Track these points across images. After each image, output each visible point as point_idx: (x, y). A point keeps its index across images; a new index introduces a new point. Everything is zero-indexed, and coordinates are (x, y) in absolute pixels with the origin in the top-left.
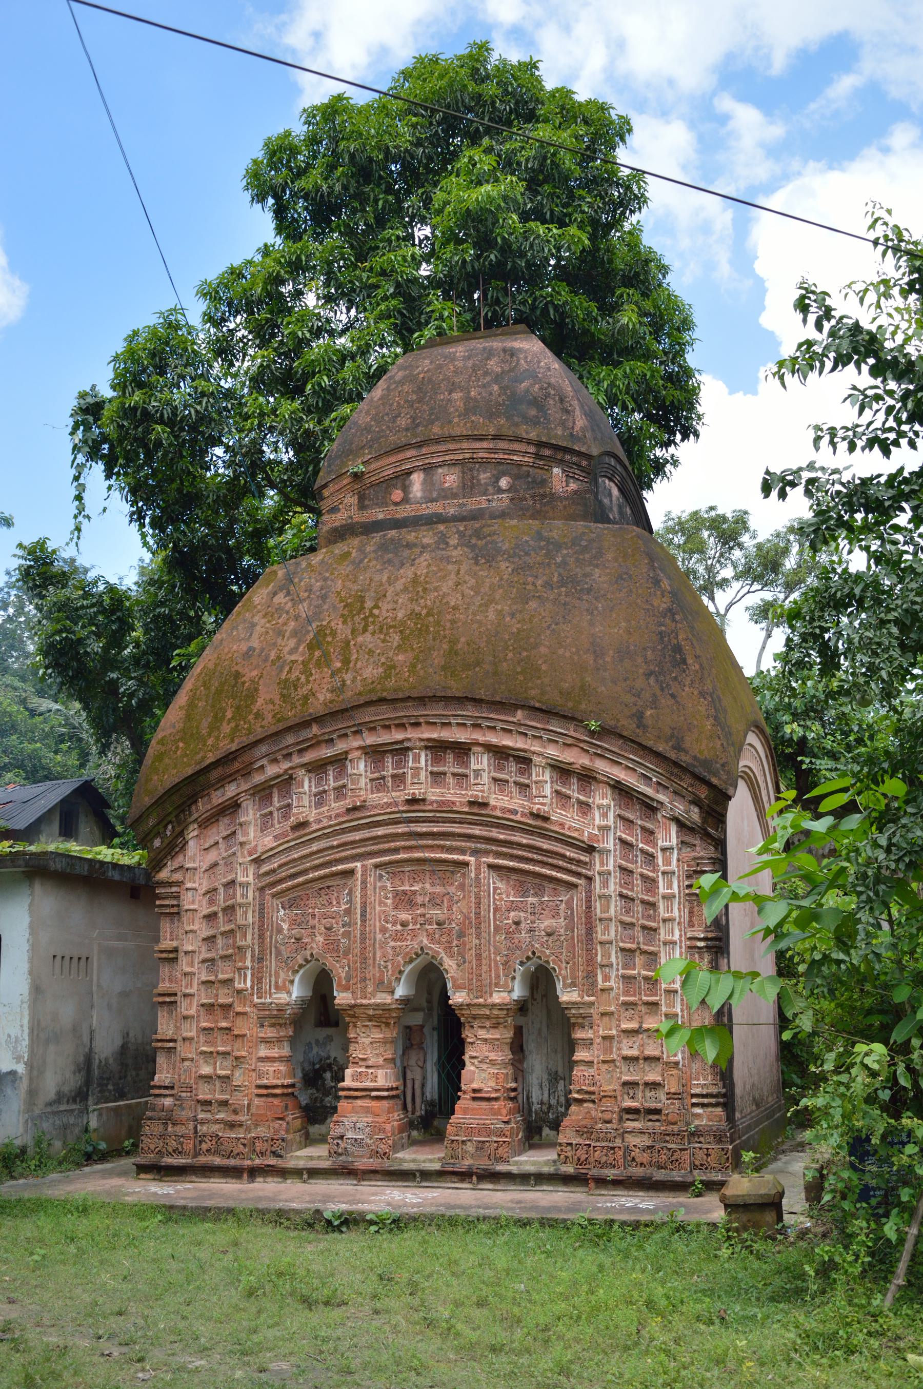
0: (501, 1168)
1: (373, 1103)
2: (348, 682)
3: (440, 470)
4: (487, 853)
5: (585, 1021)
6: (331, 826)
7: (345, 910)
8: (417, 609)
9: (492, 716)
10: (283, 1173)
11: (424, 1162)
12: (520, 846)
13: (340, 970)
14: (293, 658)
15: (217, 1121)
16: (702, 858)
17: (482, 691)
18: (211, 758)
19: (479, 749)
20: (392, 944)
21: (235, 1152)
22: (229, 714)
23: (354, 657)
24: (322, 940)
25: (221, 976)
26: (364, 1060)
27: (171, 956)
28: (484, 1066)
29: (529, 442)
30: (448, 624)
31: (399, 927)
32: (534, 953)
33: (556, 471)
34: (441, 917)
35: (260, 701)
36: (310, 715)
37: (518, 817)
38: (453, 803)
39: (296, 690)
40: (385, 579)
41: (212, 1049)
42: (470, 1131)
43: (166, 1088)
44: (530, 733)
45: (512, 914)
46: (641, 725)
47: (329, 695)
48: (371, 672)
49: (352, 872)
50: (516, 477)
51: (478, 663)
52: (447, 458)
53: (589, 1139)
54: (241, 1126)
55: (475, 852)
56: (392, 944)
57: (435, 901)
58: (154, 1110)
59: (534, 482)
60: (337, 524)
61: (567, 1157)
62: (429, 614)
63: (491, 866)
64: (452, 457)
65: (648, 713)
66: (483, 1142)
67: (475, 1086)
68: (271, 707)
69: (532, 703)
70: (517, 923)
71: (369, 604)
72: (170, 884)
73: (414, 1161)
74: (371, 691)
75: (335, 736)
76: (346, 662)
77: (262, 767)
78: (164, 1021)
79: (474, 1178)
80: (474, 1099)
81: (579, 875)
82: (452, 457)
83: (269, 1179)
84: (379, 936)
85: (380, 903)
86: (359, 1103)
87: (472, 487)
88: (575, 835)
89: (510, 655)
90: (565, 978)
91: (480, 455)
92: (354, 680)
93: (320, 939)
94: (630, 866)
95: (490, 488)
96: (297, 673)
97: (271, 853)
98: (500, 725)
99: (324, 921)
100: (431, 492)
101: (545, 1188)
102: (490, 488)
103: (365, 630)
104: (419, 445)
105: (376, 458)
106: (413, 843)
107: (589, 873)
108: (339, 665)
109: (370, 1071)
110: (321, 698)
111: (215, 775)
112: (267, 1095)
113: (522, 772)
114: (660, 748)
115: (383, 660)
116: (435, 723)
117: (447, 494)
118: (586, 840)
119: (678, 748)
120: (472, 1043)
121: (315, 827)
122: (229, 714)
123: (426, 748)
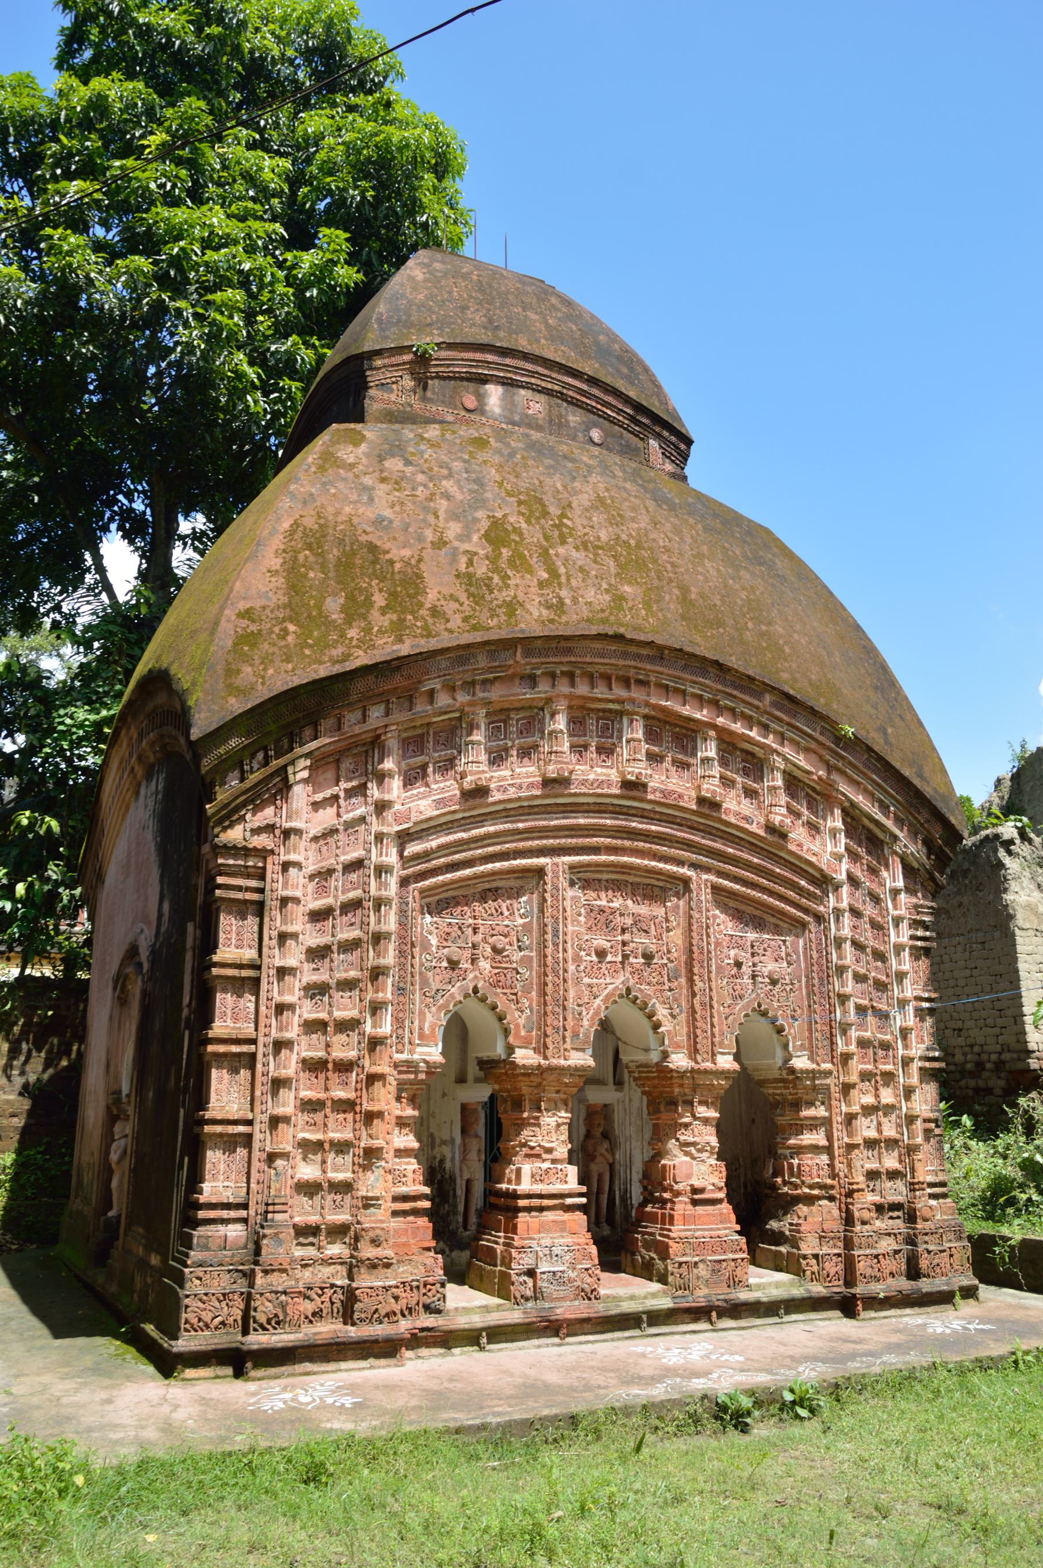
0: (743, 1295)
1: (567, 1216)
2: (568, 601)
3: (522, 392)
4: (708, 869)
5: (820, 1094)
6: (520, 799)
7: (524, 925)
8: (624, 537)
9: (735, 693)
10: (447, 1340)
11: (645, 1298)
12: (748, 866)
13: (517, 1014)
14: (466, 546)
15: (328, 1262)
16: (922, 906)
17: (733, 658)
18: (361, 659)
19: (712, 733)
20: (586, 980)
21: (383, 1312)
22: (379, 600)
23: (562, 570)
24: (488, 966)
25: (338, 1014)
26: (549, 1151)
27: (245, 973)
28: (705, 1155)
29: (627, 400)
30: (669, 567)
31: (594, 958)
32: (759, 1005)
33: (653, 443)
34: (653, 948)
35: (431, 597)
36: (522, 631)
37: (753, 828)
38: (681, 796)
39: (491, 592)
40: (559, 486)
41: (319, 1136)
42: (700, 1246)
43: (227, 1206)
44: (772, 725)
45: (732, 953)
46: (887, 742)
47: (545, 612)
48: (595, 597)
49: (540, 872)
50: (607, 434)
51: (720, 624)
52: (533, 381)
53: (835, 1246)
54: (388, 1266)
55: (694, 866)
56: (586, 980)
57: (640, 925)
58: (206, 1248)
59: (628, 446)
60: (394, 407)
61: (813, 1273)
62: (639, 546)
63: (716, 889)
64: (539, 382)
65: (890, 730)
66: (720, 1261)
67: (697, 1184)
68: (457, 605)
69: (787, 689)
70: (738, 965)
71: (554, 510)
72: (247, 852)
73: (632, 1298)
74: (604, 621)
75: (539, 672)
76: (554, 573)
77: (431, 693)
78: (224, 1087)
79: (714, 1314)
80: (695, 1203)
81: (806, 911)
82: (539, 382)
83: (424, 1351)
84: (571, 968)
85: (573, 921)
86: (549, 1216)
87: (560, 425)
88: (813, 859)
89: (750, 625)
90: (794, 1038)
91: (571, 393)
92: (575, 600)
93: (485, 965)
94: (860, 906)
95: (580, 435)
96: (484, 569)
97: (425, 826)
98: (741, 708)
99: (491, 940)
100: (512, 412)
101: (794, 1317)
102: (580, 435)
103: (563, 542)
104: (504, 352)
105: (451, 346)
106: (627, 843)
107: (822, 908)
108: (545, 575)
109: (559, 1167)
110: (536, 614)
111: (360, 686)
112: (405, 1213)
113: (746, 773)
114: (907, 772)
115: (605, 586)
116: (667, 687)
117: (530, 423)
118: (824, 867)
119: (920, 775)
120: (686, 1126)
121: (496, 796)
122: (379, 600)
123: (646, 717)
